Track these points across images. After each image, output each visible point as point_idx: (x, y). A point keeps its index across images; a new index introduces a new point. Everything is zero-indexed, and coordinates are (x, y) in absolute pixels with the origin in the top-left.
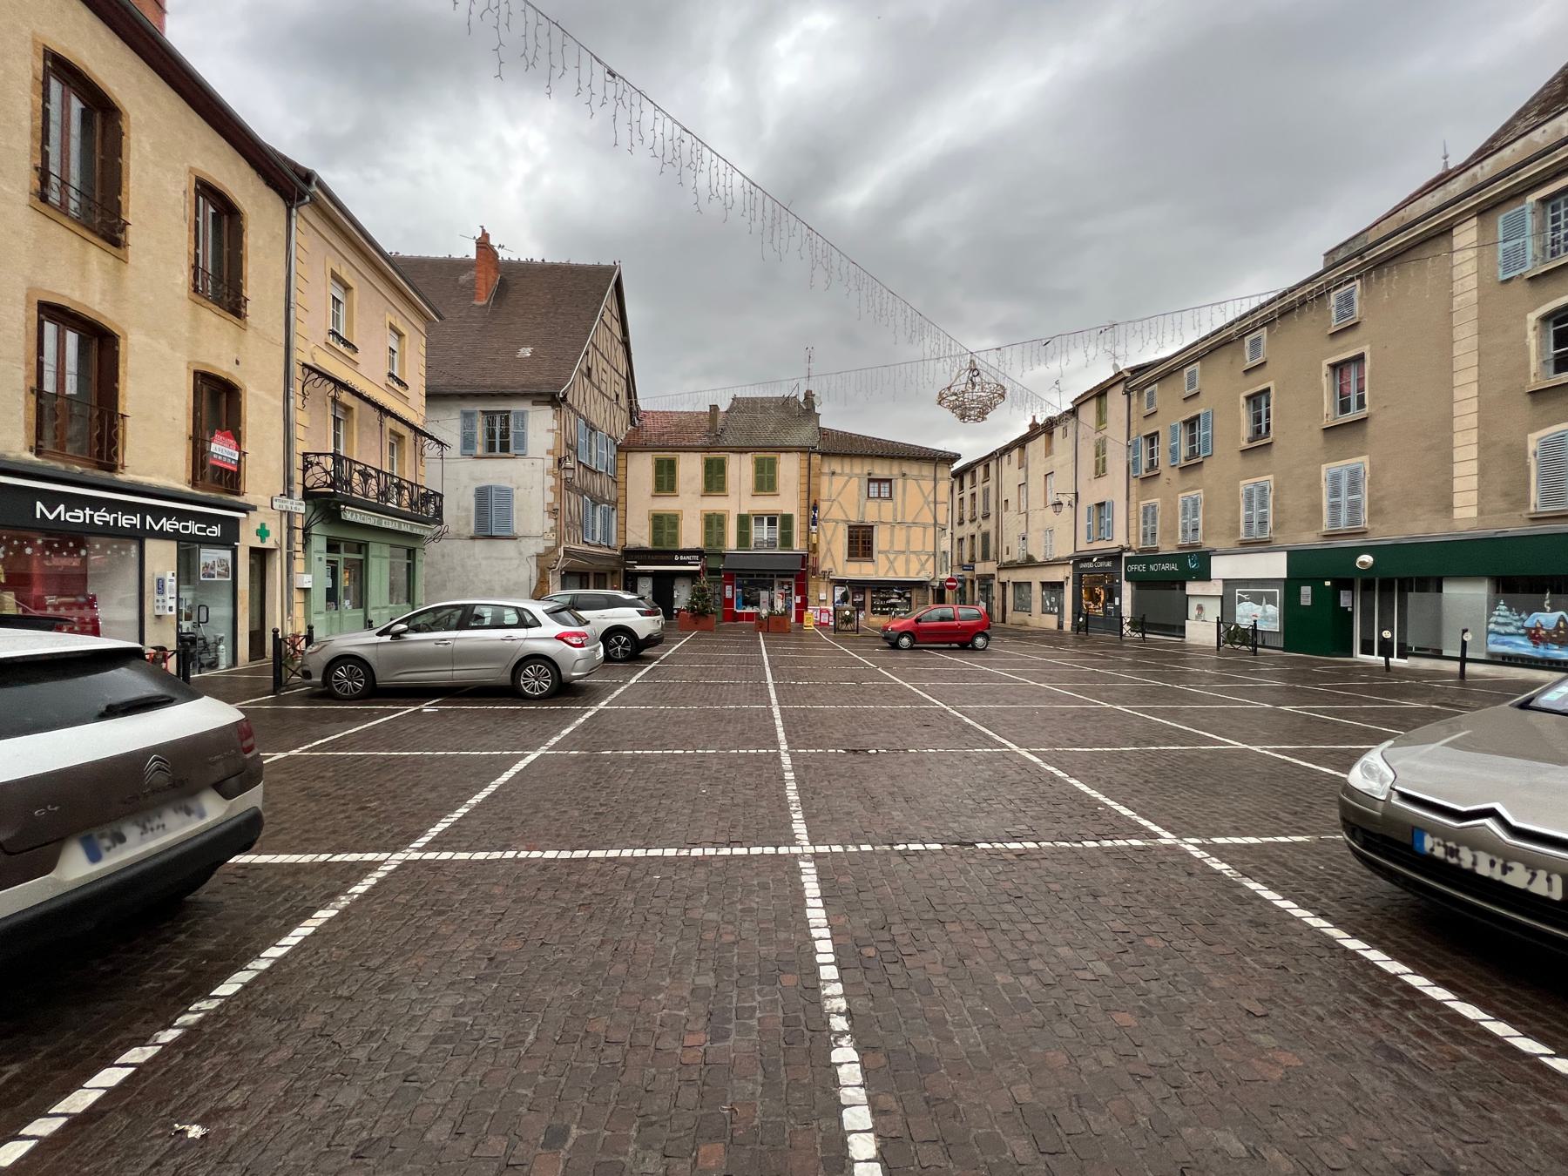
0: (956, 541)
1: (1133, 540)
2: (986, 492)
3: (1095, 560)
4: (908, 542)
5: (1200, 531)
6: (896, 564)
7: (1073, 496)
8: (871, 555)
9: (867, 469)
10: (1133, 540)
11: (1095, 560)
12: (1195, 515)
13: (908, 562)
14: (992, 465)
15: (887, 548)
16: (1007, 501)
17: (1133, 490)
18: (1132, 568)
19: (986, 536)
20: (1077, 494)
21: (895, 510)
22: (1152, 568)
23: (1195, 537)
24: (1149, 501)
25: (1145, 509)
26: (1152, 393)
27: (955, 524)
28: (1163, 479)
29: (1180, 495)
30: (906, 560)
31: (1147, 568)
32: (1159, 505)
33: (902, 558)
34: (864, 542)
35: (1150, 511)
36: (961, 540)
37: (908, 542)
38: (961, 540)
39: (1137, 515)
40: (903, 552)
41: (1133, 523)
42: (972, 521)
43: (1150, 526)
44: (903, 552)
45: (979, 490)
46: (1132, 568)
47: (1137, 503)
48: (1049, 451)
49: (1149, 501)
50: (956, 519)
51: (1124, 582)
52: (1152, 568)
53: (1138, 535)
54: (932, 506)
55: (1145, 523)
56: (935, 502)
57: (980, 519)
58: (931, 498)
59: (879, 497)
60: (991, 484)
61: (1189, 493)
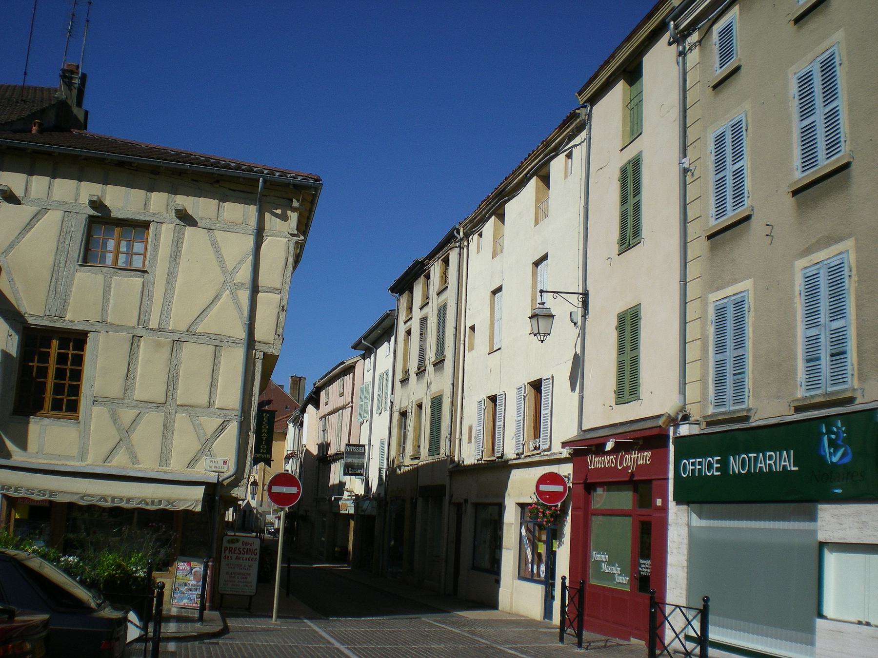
0: (396, 416)
1: (693, 392)
2: (442, 311)
3: (609, 446)
4: (172, 381)
5: (852, 356)
6: (136, 436)
7: (576, 300)
8: (73, 407)
9: (89, 190)
10: (693, 392)
11: (609, 446)
12: (837, 312)
13: (167, 428)
14: (454, 256)
15: (114, 389)
16: (473, 328)
17: (693, 270)
18: (691, 466)
19: (437, 403)
20: (585, 295)
21: (145, 292)
22: (735, 465)
23: (838, 377)
24: (729, 291)
25: (721, 312)
26: (727, 32)
27: (398, 384)
28: (757, 226)
29: (800, 263)
30: (165, 426)
31: (724, 465)
32: (750, 300)
33: (153, 421)
34: (60, 374)
35: (730, 313)
36: (403, 414)
37: (172, 381)
38: (403, 414)
39: (704, 328)
40: (159, 405)
41: (693, 352)
42: (421, 372)
43: (730, 353)
44: (159, 405)
45: (431, 311)
46: (691, 466)
47: (702, 298)
48: (541, 213)
49: (729, 291)
50: (399, 376)
51: (672, 504)
52: (735, 465)
53: (703, 380)
54: (244, 296)
55: (720, 347)
56: (255, 289)
57: (430, 369)
58: (244, 274)
59: (115, 266)
60: (450, 295)
61: (820, 255)
